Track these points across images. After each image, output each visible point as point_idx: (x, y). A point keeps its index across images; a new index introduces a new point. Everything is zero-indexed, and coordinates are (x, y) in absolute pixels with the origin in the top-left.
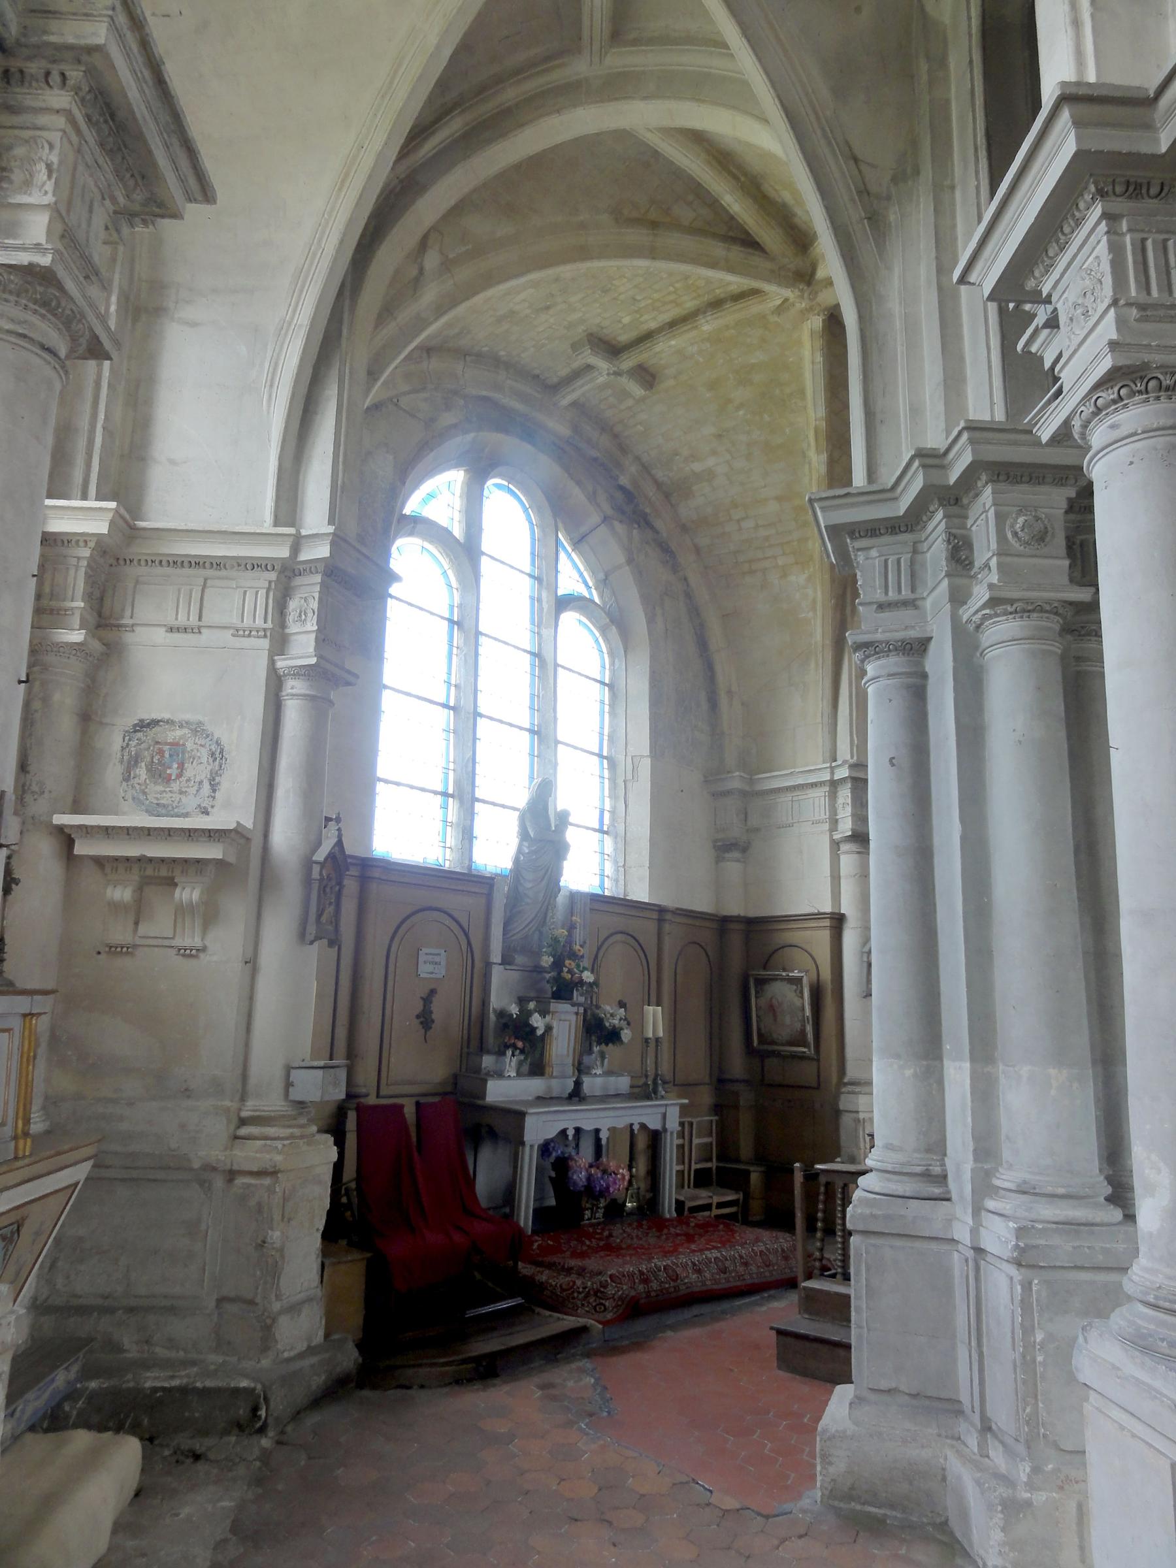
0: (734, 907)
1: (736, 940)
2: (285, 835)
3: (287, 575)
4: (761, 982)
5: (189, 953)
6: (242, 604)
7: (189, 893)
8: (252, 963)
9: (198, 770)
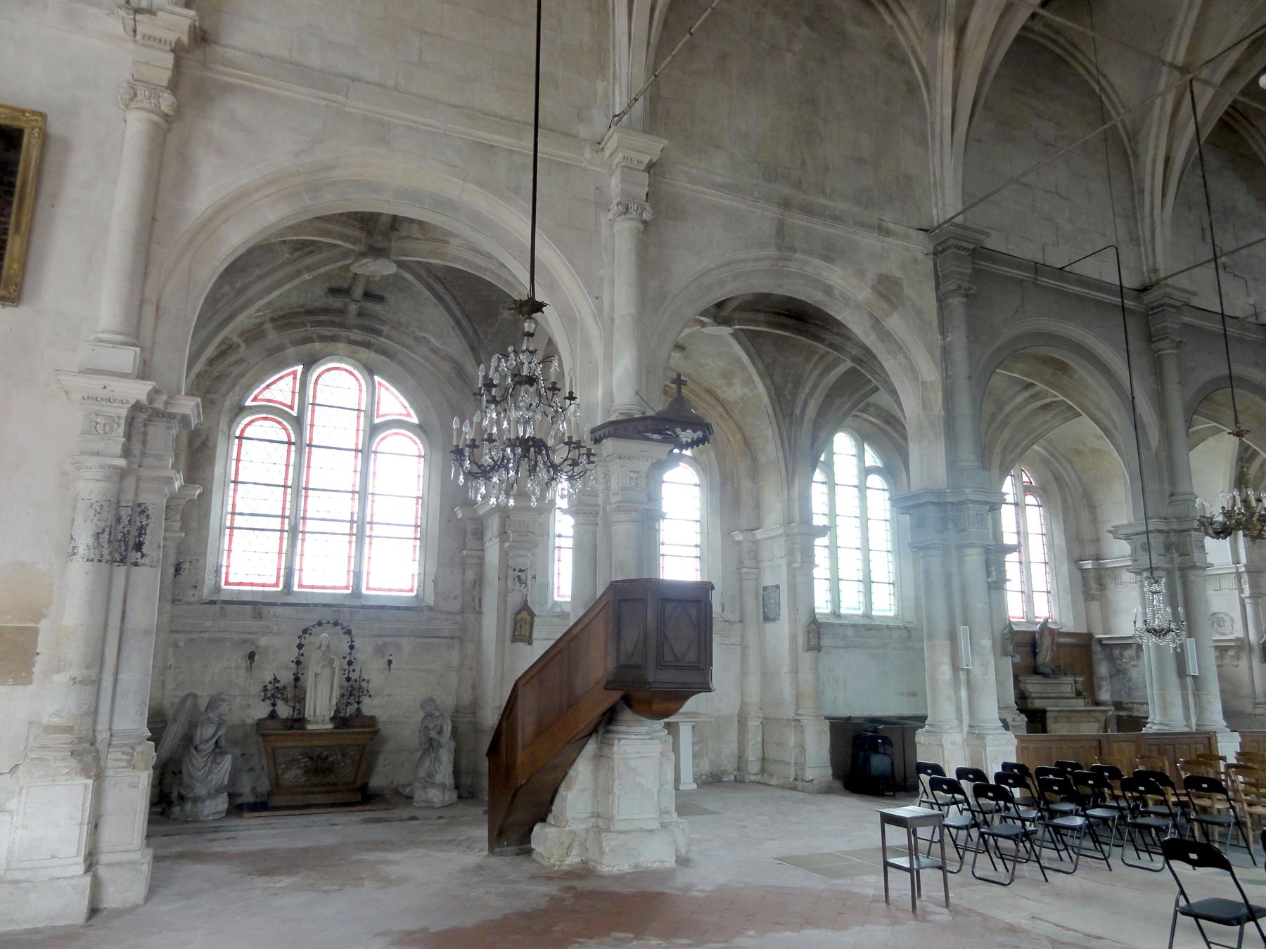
2: (1253, 637)
6: (1231, 582)
7: (1231, 653)
8: (1251, 668)
9: (1228, 623)
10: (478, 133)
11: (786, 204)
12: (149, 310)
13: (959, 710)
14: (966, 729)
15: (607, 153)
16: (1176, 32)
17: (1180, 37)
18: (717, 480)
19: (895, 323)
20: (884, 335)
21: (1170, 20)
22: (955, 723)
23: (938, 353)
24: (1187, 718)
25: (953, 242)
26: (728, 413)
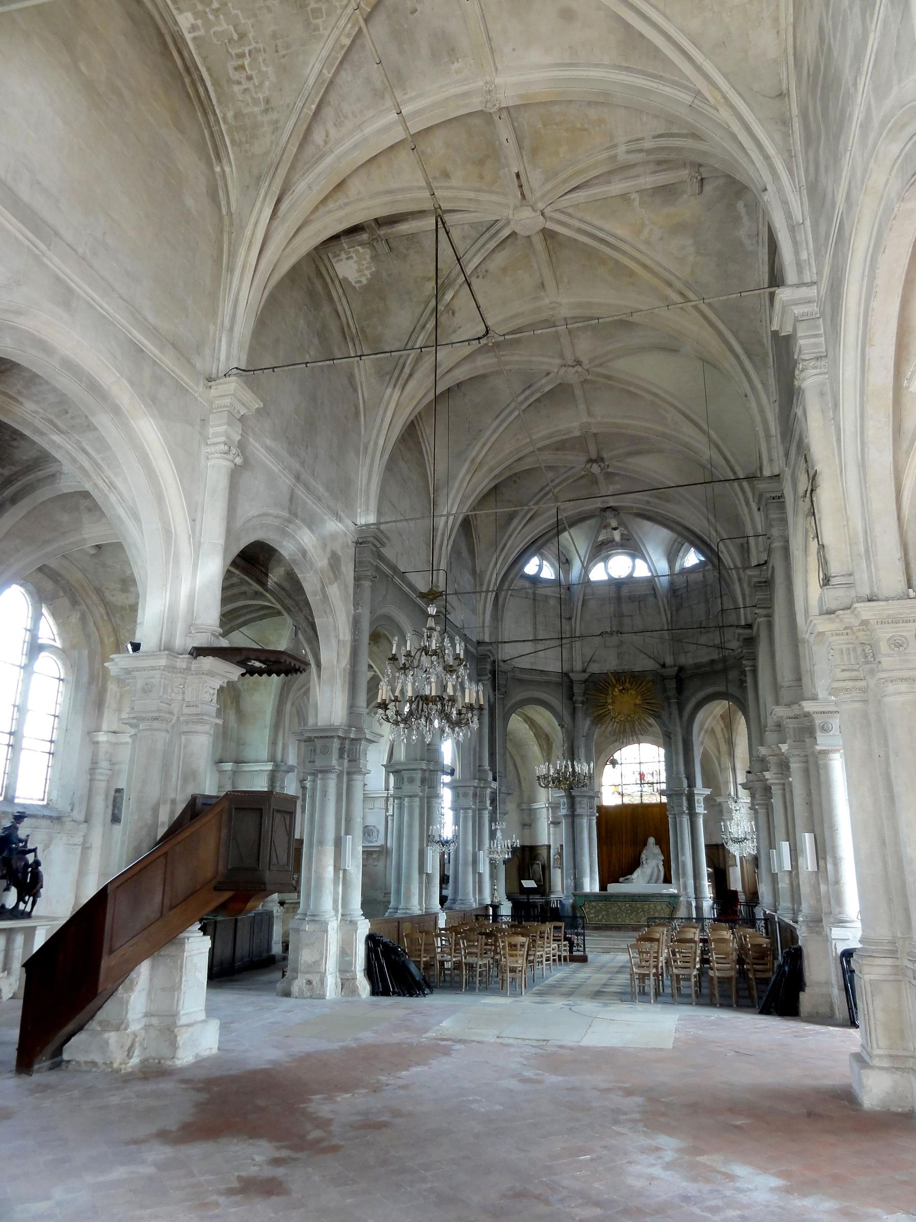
0: (527, 843)
1: (527, 853)
3: (387, 798)
4: (532, 865)
5: (375, 866)
6: (381, 804)
7: (374, 856)
8: (385, 867)
9: (375, 834)
10: (135, 332)
11: (298, 478)
12: (389, 572)
13: (335, 901)
14: (340, 916)
15: (213, 392)
16: (483, 440)
17: (484, 444)
18: (85, 678)
19: (334, 591)
20: (325, 598)
21: (481, 431)
22: (333, 913)
23: (351, 619)
24: (420, 903)
25: (371, 539)
26: (108, 614)
